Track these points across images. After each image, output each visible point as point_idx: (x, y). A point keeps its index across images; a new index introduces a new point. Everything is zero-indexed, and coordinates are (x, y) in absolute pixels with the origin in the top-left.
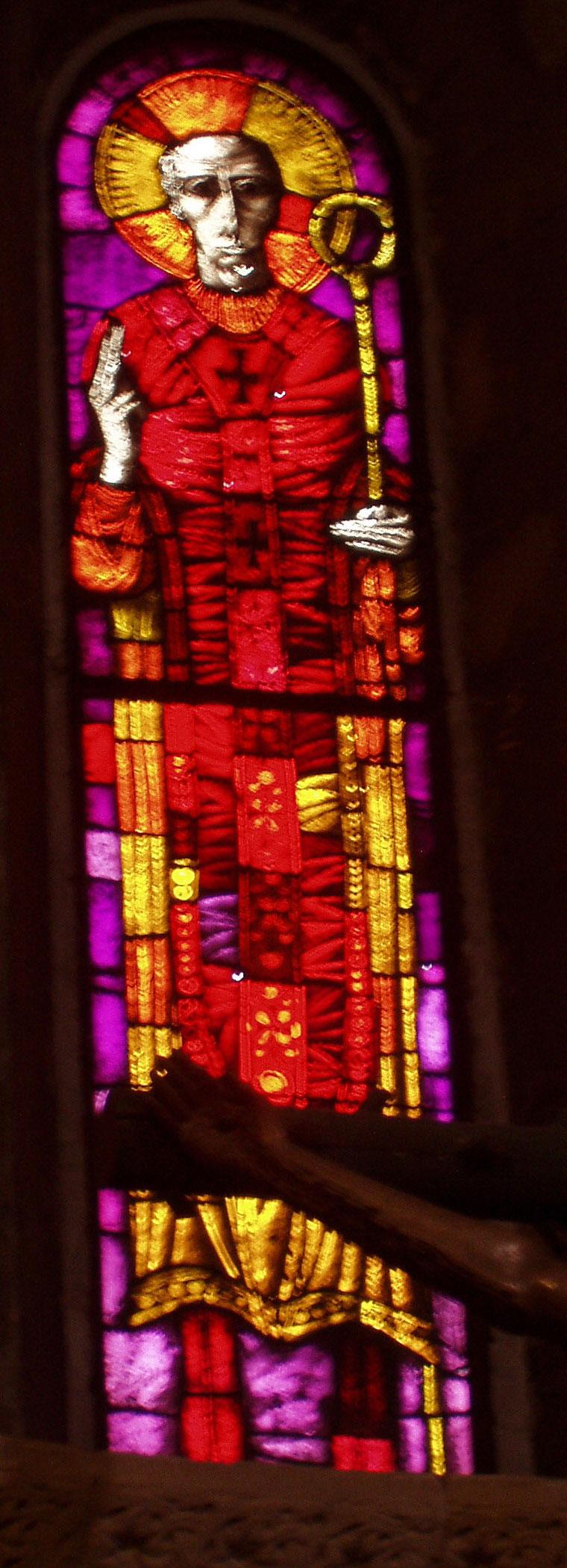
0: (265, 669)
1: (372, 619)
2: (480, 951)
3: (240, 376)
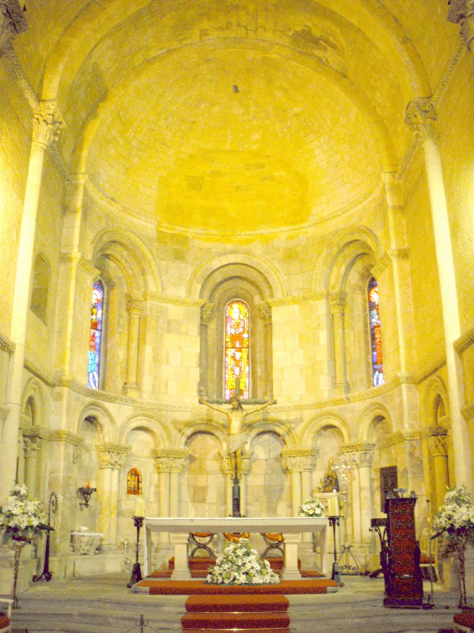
0: (238, 345)
1: (245, 342)
2: (250, 364)
3: (237, 325)
